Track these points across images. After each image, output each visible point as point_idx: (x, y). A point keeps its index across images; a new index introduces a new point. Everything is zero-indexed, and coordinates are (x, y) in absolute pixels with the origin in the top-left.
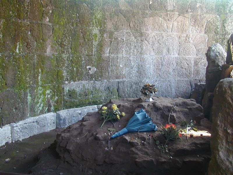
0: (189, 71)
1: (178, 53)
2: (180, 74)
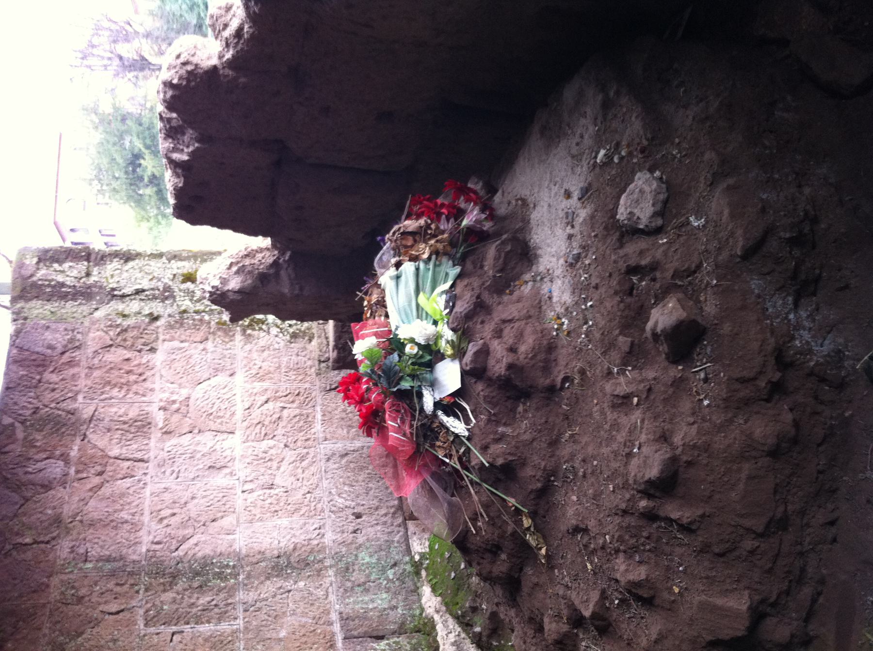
1: (225, 436)
2: (301, 423)
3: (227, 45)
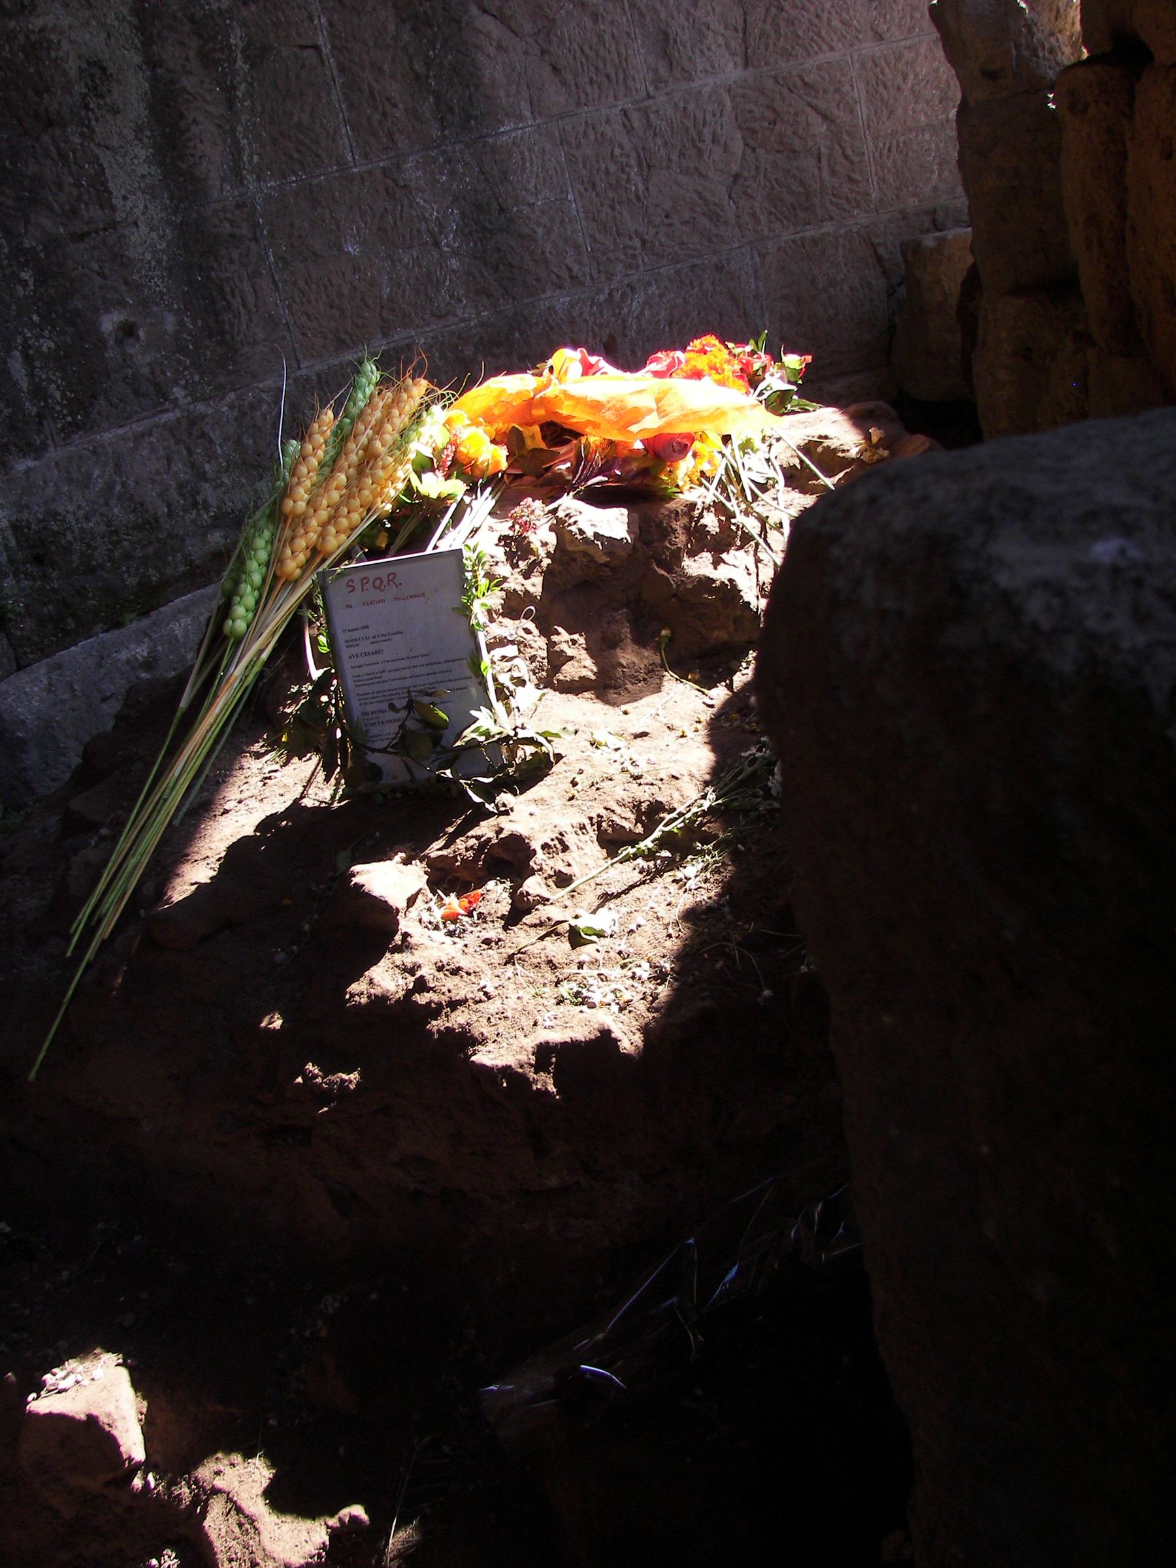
1: (740, 49)
2: (789, 199)
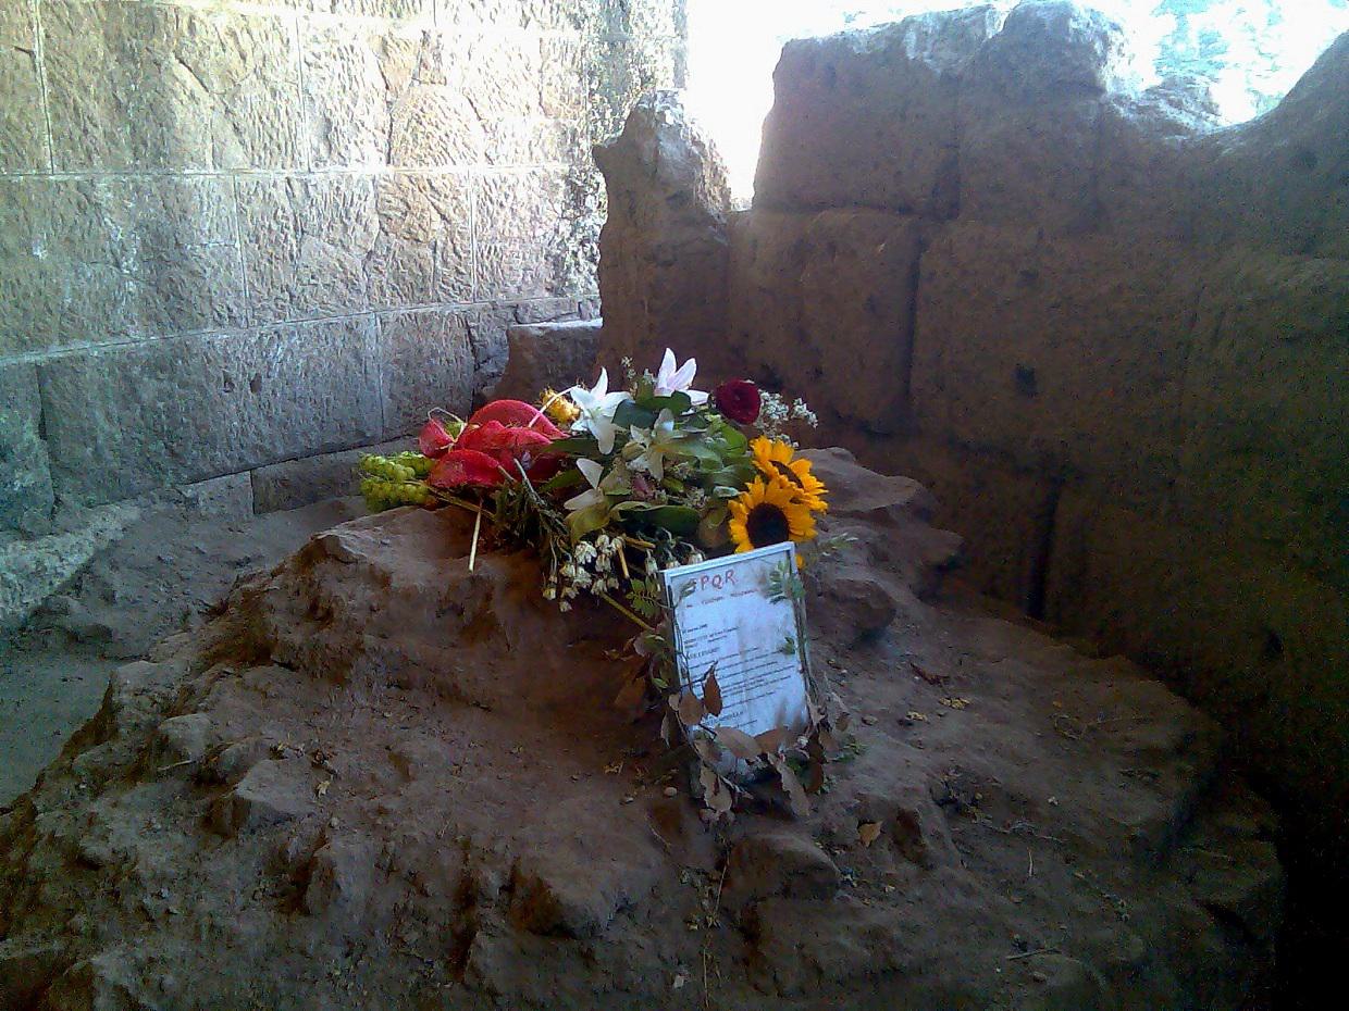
0: (452, 259)
3: (1141, 110)
